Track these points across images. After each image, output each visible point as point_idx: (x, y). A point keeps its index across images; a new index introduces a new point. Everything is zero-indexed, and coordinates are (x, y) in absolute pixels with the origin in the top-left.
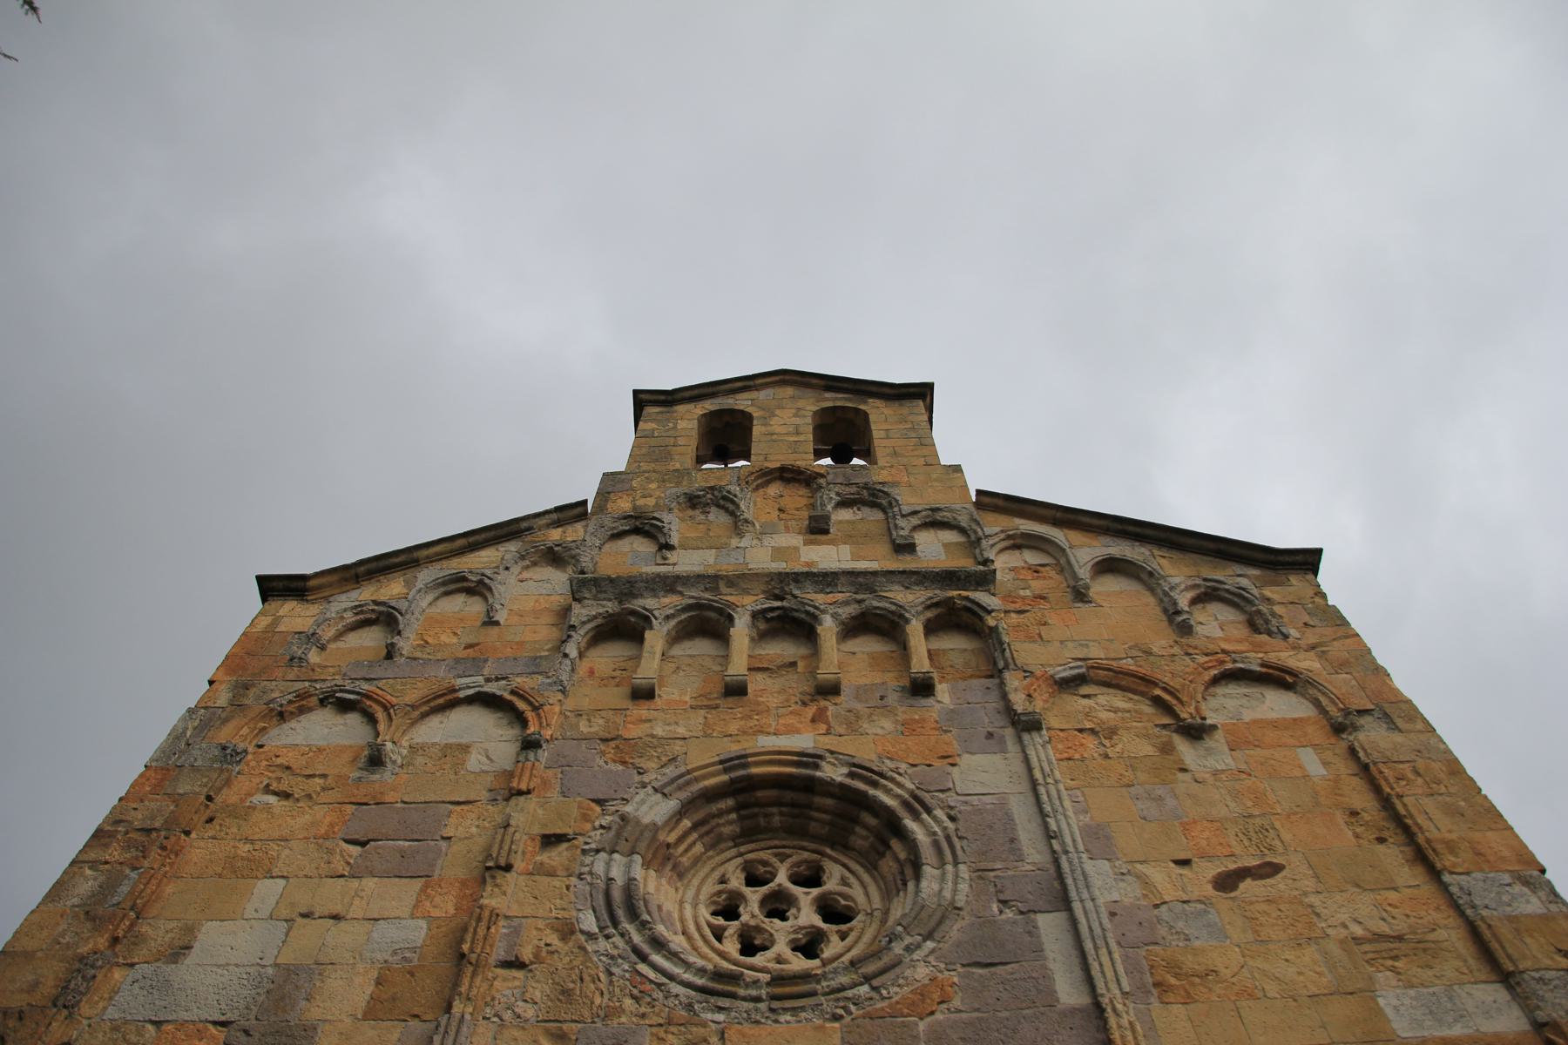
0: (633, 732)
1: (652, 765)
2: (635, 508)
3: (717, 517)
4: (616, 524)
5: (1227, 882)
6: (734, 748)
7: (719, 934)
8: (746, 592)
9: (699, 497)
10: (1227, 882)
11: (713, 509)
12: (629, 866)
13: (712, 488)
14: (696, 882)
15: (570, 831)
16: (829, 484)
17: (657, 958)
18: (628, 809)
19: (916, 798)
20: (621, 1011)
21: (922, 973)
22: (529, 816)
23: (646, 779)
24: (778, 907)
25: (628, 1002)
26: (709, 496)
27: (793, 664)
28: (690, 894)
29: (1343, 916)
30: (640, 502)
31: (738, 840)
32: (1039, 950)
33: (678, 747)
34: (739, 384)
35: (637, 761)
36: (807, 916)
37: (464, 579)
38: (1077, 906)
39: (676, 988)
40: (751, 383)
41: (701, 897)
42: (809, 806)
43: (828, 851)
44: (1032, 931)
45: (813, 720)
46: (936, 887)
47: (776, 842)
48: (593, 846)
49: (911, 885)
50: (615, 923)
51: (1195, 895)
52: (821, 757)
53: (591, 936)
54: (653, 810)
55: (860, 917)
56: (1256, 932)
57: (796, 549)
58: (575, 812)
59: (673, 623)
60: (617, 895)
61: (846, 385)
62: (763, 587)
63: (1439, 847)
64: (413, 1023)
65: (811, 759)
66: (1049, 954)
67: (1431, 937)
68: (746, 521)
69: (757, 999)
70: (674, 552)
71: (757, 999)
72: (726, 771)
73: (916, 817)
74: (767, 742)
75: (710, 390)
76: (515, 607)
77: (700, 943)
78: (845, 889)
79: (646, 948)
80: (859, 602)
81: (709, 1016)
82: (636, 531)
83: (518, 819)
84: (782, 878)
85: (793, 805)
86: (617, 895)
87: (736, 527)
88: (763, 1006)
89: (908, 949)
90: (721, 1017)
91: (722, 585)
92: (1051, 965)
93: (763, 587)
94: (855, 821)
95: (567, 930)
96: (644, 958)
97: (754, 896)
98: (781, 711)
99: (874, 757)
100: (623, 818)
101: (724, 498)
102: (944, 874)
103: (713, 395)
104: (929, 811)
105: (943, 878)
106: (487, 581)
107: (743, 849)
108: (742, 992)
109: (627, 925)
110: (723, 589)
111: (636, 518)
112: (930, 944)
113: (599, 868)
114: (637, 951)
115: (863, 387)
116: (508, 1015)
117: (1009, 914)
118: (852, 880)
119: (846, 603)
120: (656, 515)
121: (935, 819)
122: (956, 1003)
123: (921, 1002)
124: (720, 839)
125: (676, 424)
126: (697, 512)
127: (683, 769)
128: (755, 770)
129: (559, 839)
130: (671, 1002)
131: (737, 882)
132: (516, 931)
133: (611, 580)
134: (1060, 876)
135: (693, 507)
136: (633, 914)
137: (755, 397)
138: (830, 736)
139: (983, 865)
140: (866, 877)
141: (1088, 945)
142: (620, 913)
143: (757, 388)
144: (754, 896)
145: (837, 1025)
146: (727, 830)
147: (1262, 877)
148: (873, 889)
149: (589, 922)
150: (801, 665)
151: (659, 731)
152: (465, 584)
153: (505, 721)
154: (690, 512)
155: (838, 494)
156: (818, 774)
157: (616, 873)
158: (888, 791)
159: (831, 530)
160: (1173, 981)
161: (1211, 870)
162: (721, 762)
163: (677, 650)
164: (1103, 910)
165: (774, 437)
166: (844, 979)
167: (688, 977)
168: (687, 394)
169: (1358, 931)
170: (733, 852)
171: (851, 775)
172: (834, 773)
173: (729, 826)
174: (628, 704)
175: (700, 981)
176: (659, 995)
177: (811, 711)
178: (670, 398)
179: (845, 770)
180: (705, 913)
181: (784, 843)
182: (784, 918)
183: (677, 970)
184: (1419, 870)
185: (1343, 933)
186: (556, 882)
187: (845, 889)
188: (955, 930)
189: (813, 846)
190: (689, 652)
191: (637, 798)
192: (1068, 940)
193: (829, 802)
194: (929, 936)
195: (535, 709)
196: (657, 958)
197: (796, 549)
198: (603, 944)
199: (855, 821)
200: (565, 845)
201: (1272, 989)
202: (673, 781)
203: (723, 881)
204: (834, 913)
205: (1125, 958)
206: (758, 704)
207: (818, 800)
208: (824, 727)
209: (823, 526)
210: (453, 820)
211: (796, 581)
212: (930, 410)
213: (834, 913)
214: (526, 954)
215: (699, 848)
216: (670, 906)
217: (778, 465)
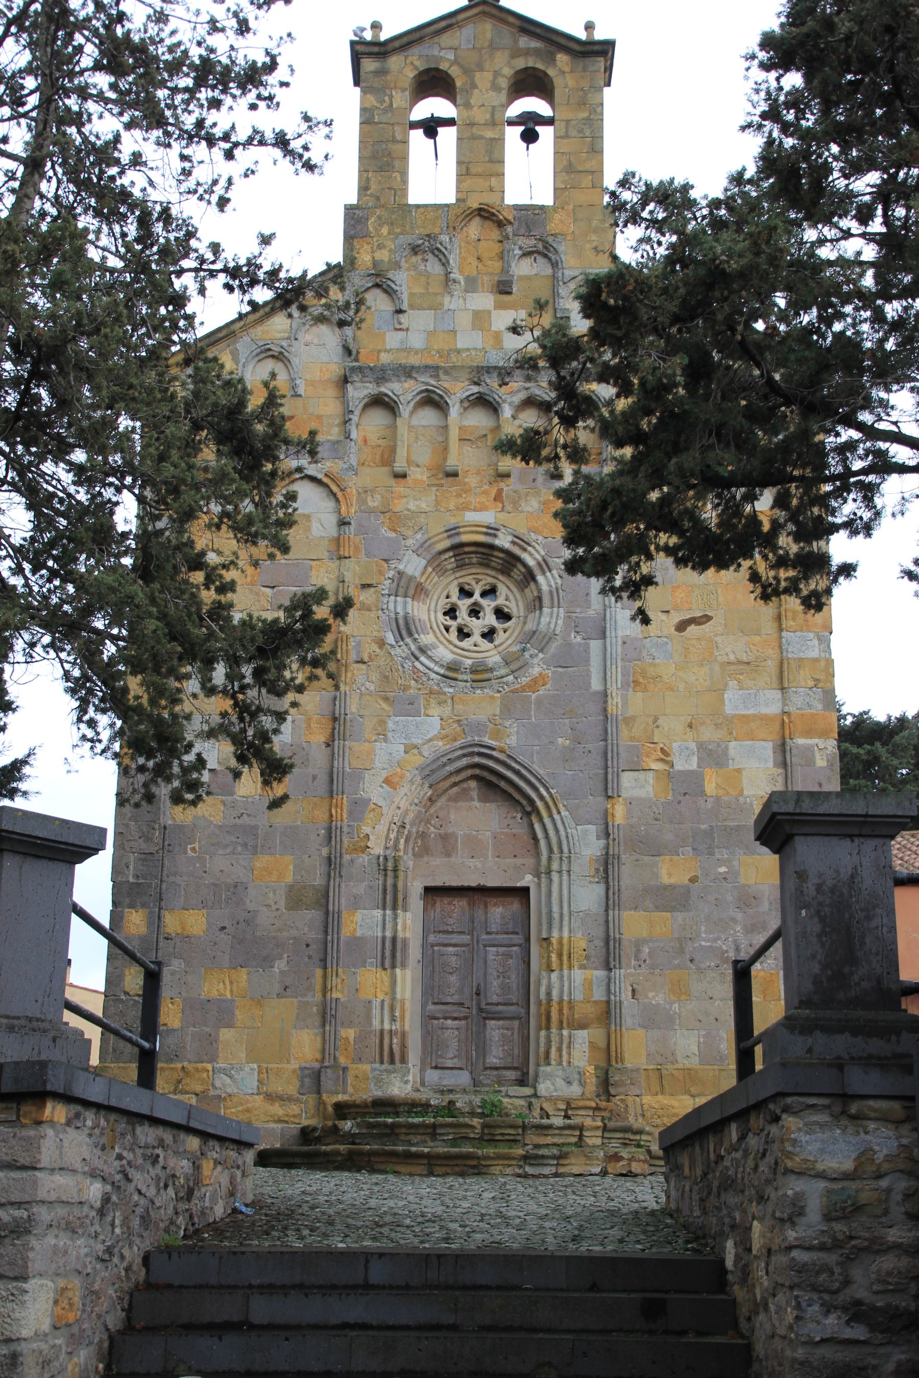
0: (398, 506)
1: (409, 533)
2: (375, 263)
3: (433, 267)
4: (363, 282)
5: (682, 626)
6: (452, 521)
7: (447, 629)
8: (456, 379)
9: (419, 246)
10: (682, 626)
11: (430, 257)
12: (405, 603)
13: (428, 236)
14: (435, 598)
15: (374, 582)
16: (514, 235)
17: (423, 659)
18: (401, 567)
19: (544, 560)
20: (409, 687)
21: (536, 671)
22: (353, 571)
23: (410, 542)
24: (475, 612)
25: (413, 682)
26: (427, 244)
27: (485, 436)
28: (433, 605)
29: (728, 650)
30: (378, 255)
31: (453, 570)
32: (587, 661)
33: (422, 519)
34: (443, 24)
35: (402, 529)
36: (490, 619)
37: (270, 350)
38: (608, 640)
39: (433, 676)
40: (453, 20)
41: (439, 608)
42: (492, 555)
43: (500, 577)
44: (587, 650)
45: (495, 499)
46: (548, 620)
47: (474, 571)
48: (387, 592)
49: (537, 612)
50: (403, 639)
51: (665, 633)
52: (497, 530)
53: (392, 646)
54: (413, 565)
55: (513, 620)
56: (686, 657)
57: (489, 312)
58: (375, 569)
59: (412, 404)
60: (401, 622)
61: (538, 31)
62: (467, 376)
63: (789, 614)
64: (323, 692)
65: (492, 530)
66: (592, 663)
67: (763, 664)
68: (454, 281)
69: (466, 681)
70: (406, 315)
71: (466, 681)
72: (449, 537)
73: (544, 573)
74: (472, 517)
75: (418, 35)
76: (308, 377)
77: (439, 635)
78: (507, 603)
79: (417, 653)
80: (527, 389)
81: (446, 690)
82: (377, 286)
83: (348, 577)
84: (477, 596)
85: (483, 553)
86: (401, 622)
87: (447, 285)
88: (468, 684)
89: (531, 656)
90: (451, 690)
91: (441, 372)
92: (592, 669)
93: (467, 376)
94: (515, 566)
95: (382, 643)
96: (417, 659)
97: (464, 605)
98: (478, 490)
99: (525, 532)
100: (400, 574)
101: (438, 249)
102: (552, 613)
103: (420, 40)
104: (550, 571)
105: (551, 617)
106: (286, 354)
107: (458, 575)
108: (460, 677)
109: (408, 640)
110: (442, 376)
111: (377, 275)
112: (541, 655)
113: (391, 606)
114: (413, 654)
115: (554, 38)
116: (363, 689)
117: (579, 639)
118: (511, 597)
119: (519, 391)
120: (390, 275)
121: (552, 575)
122: (548, 686)
123: (534, 684)
124: (446, 571)
125: (391, 97)
126: (420, 257)
127: (426, 537)
128: (465, 538)
129: (369, 586)
130: (431, 682)
131: (454, 598)
132: (359, 644)
133: (371, 369)
134: (605, 619)
135: (416, 254)
136: (410, 634)
137: (456, 43)
138: (503, 514)
139: (572, 609)
140: (518, 595)
141: (608, 663)
142: (404, 632)
143: (459, 25)
144: (464, 605)
145: (498, 695)
146: (449, 567)
147: (700, 624)
148: (521, 604)
149: (390, 638)
150: (489, 437)
151: (412, 506)
152: (271, 353)
153: (325, 494)
154: (414, 259)
155: (521, 248)
156: (497, 542)
157: (399, 609)
158: (531, 555)
159: (514, 290)
160: (641, 680)
161: (676, 618)
162: (446, 531)
163: (415, 422)
164: (619, 639)
165: (475, 130)
166: (503, 672)
167: (436, 668)
168: (397, 44)
169: (732, 658)
170: (453, 577)
171: (513, 543)
172: (504, 541)
173: (451, 563)
174: (392, 482)
175: (442, 671)
176: (425, 679)
177: (494, 492)
178: (382, 49)
179: (510, 538)
180: (441, 617)
181: (479, 571)
182: (478, 618)
183: (432, 665)
184: (776, 625)
185: (725, 659)
186: (373, 615)
187: (507, 603)
188: (553, 647)
189: (493, 573)
190: (424, 423)
191: (406, 558)
192: (600, 657)
193: (501, 555)
194: (541, 651)
195: (342, 490)
196: (423, 659)
197: (489, 312)
198: (398, 651)
199: (515, 566)
200: (372, 589)
201: (681, 687)
202: (422, 546)
203: (448, 597)
204: (502, 615)
205: (623, 668)
206: (465, 484)
207: (496, 553)
208: (500, 505)
209: (508, 289)
210: (314, 573)
211: (488, 372)
212: (609, 69)
213: (502, 615)
214: (366, 659)
215: (436, 579)
216: (424, 616)
217: (475, 206)
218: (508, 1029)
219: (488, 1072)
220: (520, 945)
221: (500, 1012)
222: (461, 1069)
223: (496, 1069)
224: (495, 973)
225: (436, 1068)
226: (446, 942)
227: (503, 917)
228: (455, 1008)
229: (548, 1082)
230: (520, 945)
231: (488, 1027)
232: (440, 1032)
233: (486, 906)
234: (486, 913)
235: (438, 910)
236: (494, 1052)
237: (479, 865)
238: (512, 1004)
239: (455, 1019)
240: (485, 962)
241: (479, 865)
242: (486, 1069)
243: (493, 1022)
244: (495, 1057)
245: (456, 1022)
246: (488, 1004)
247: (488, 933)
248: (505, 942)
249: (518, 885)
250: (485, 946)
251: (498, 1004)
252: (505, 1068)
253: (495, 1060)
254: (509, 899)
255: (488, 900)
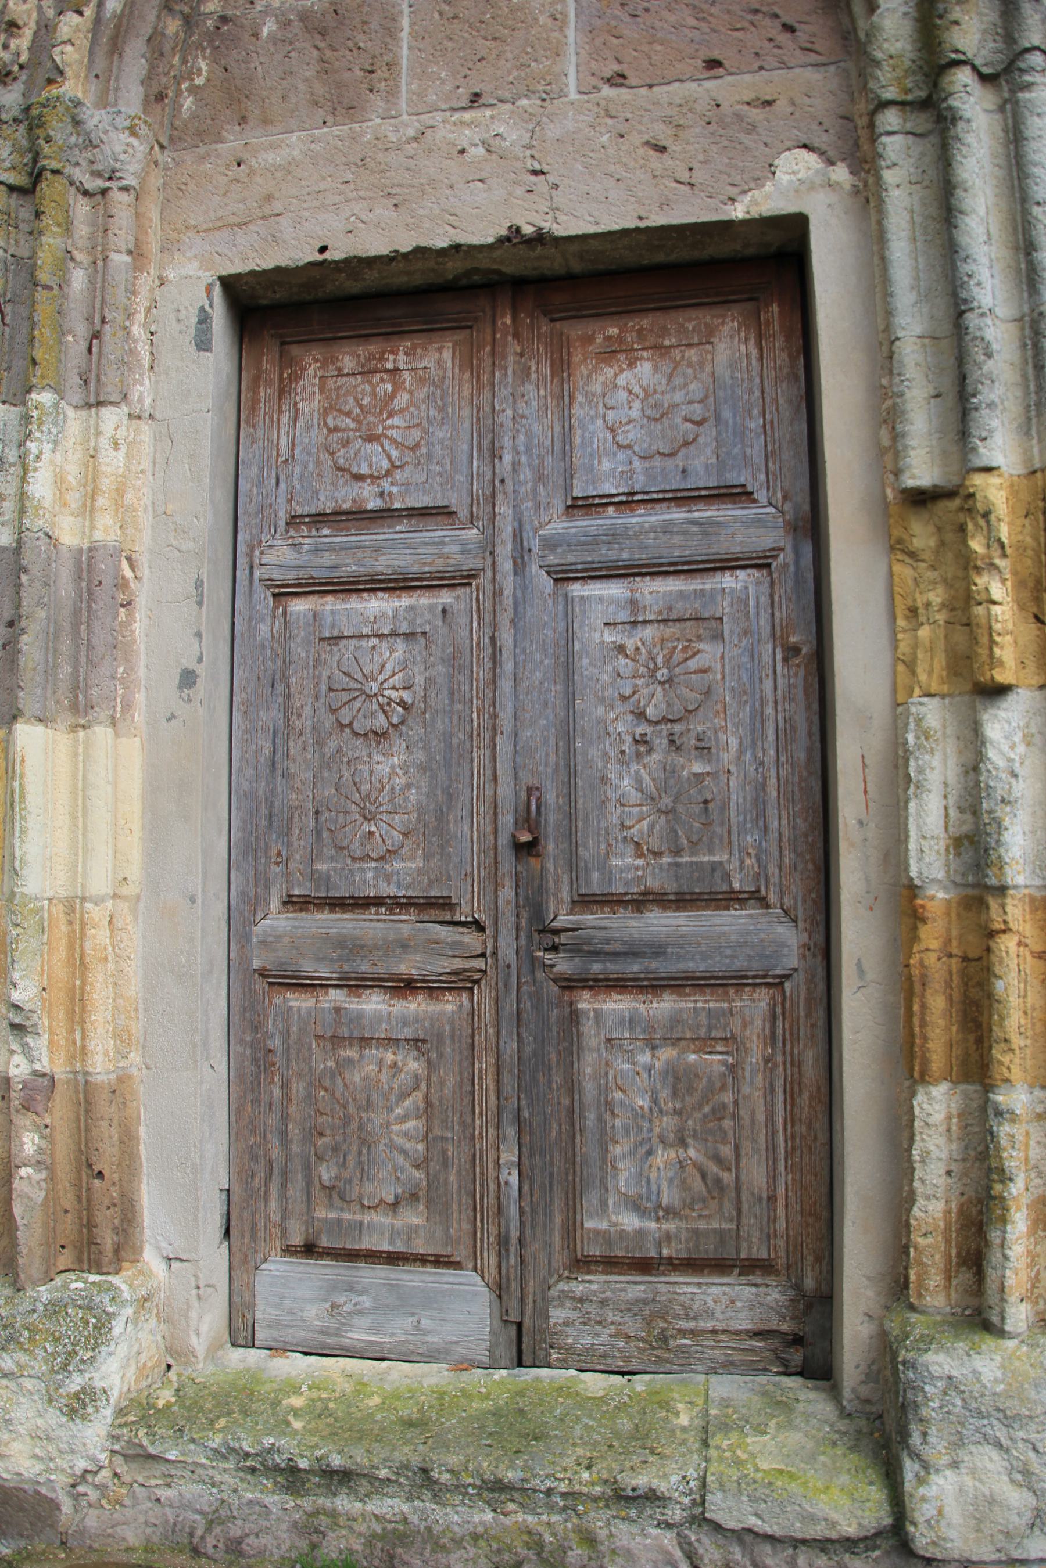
218: (705, 1044)
219: (592, 1284)
220: (761, 563)
221: (658, 949)
222: (439, 1261)
223: (644, 1266)
224: (623, 726)
225: (309, 1250)
226: (351, 568)
227: (658, 415)
228: (406, 924)
229: (989, 1460)
230: (761, 563)
231: (591, 1035)
232: (323, 1062)
233: (562, 367)
234: (564, 401)
235: (310, 406)
236: (624, 1178)
237: (513, 135)
238: (731, 899)
239: (406, 987)
240: (567, 668)
241: (513, 135)
242: (582, 1264)
243: (617, 1005)
244: (636, 1206)
245: (415, 1006)
246: (585, 902)
247: (580, 506)
248: (679, 548)
249: (738, 212)
250: (562, 577)
251: (641, 902)
252: (691, 1265)
253: (630, 1221)
254: (691, 320)
255: (575, 330)
